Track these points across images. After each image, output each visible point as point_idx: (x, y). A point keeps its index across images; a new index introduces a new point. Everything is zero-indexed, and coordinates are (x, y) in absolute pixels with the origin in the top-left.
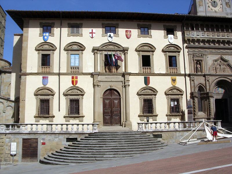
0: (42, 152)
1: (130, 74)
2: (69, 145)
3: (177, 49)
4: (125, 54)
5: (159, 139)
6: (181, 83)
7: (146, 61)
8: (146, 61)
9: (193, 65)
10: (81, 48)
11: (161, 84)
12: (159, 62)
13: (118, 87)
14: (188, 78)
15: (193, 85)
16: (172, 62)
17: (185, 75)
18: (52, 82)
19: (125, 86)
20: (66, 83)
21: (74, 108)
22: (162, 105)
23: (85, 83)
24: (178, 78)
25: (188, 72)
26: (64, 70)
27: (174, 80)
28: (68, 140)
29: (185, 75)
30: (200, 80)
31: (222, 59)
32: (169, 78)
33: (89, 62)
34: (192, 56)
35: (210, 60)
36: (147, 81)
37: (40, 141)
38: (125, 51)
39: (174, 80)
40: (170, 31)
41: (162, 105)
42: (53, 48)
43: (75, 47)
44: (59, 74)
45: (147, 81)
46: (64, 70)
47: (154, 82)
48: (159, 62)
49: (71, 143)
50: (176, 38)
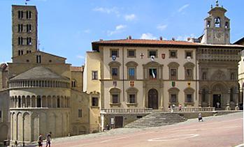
3: (192, 65)
6: (194, 85)
7: (173, 74)
8: (173, 74)
10: (136, 65)
11: (182, 86)
12: (181, 73)
13: (157, 87)
14: (198, 82)
16: (189, 73)
17: (196, 81)
18: (119, 85)
20: (128, 85)
21: (132, 98)
22: (181, 97)
23: (139, 86)
24: (192, 82)
25: (198, 79)
26: (126, 78)
27: (189, 84)
29: (196, 81)
30: (205, 83)
31: (219, 71)
32: (187, 82)
34: (201, 69)
35: (212, 72)
36: (173, 84)
38: (162, 66)
39: (189, 84)
40: (189, 54)
41: (181, 97)
42: (119, 64)
45: (173, 84)
46: (126, 78)
47: (178, 84)
48: (181, 73)
50: (192, 58)
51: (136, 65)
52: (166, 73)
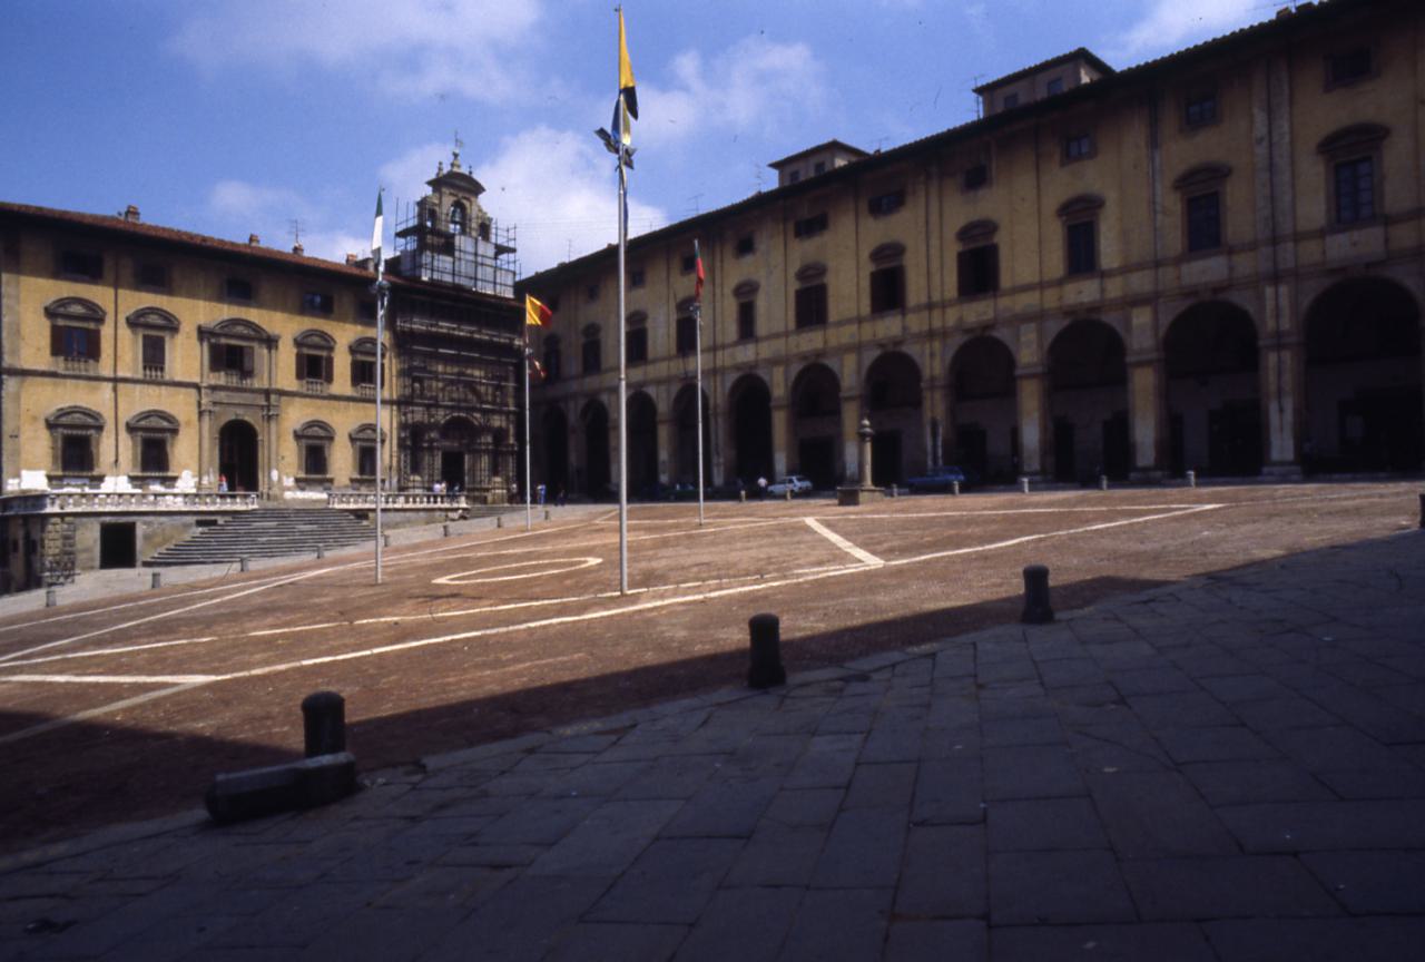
0: (143, 550)
1: (282, 393)
2: (202, 533)
4: (270, 348)
5: (365, 523)
11: (344, 421)
14: (395, 408)
19: (269, 418)
22: (342, 461)
28: (199, 523)
33: (186, 357)
37: (140, 530)
38: (271, 342)
41: (342, 461)
43: (154, 319)
44: (116, 380)
49: (205, 529)
51: (171, 325)
52: (281, 368)
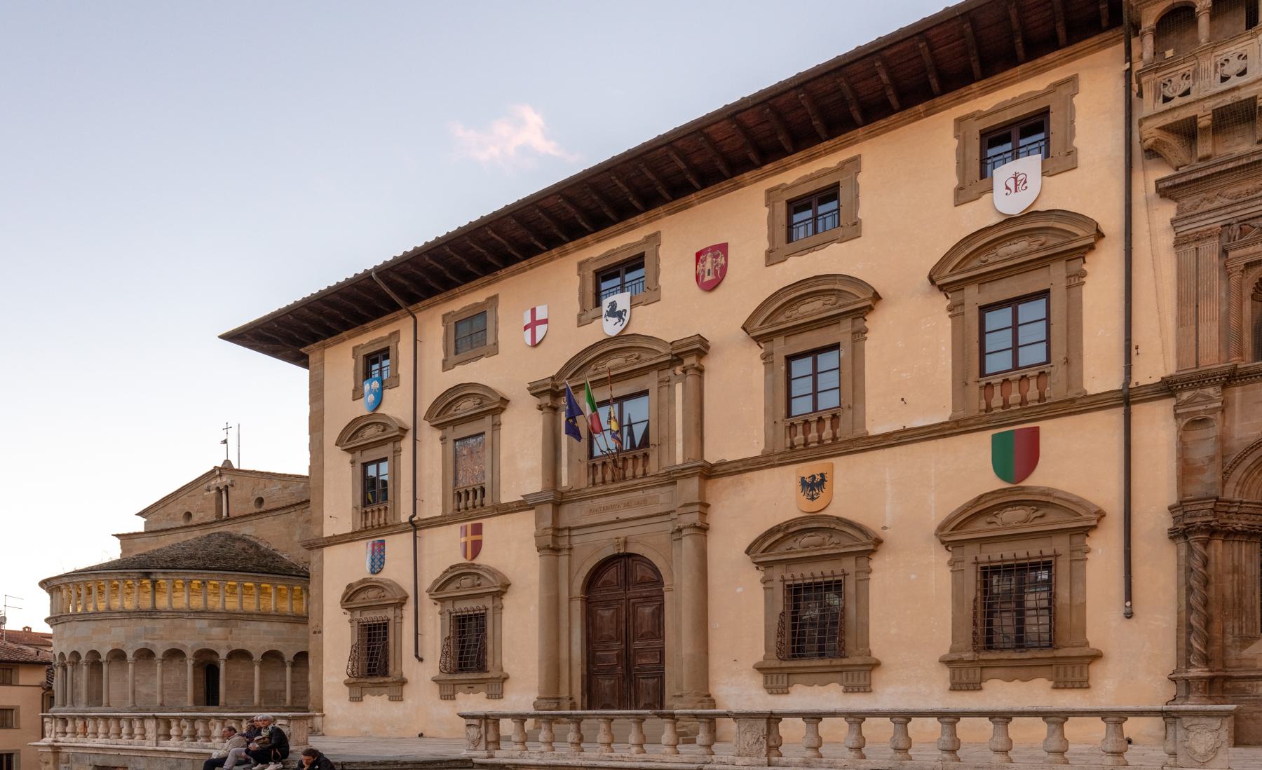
9: (1212, 310)
15: (1203, 450)
25: (1155, 364)
